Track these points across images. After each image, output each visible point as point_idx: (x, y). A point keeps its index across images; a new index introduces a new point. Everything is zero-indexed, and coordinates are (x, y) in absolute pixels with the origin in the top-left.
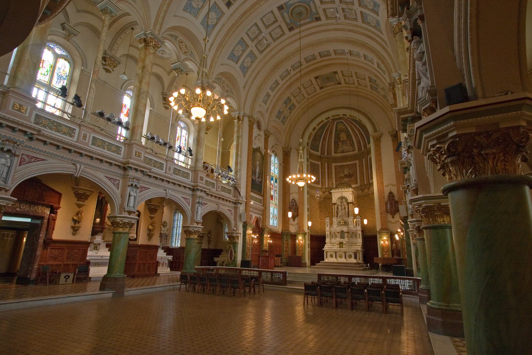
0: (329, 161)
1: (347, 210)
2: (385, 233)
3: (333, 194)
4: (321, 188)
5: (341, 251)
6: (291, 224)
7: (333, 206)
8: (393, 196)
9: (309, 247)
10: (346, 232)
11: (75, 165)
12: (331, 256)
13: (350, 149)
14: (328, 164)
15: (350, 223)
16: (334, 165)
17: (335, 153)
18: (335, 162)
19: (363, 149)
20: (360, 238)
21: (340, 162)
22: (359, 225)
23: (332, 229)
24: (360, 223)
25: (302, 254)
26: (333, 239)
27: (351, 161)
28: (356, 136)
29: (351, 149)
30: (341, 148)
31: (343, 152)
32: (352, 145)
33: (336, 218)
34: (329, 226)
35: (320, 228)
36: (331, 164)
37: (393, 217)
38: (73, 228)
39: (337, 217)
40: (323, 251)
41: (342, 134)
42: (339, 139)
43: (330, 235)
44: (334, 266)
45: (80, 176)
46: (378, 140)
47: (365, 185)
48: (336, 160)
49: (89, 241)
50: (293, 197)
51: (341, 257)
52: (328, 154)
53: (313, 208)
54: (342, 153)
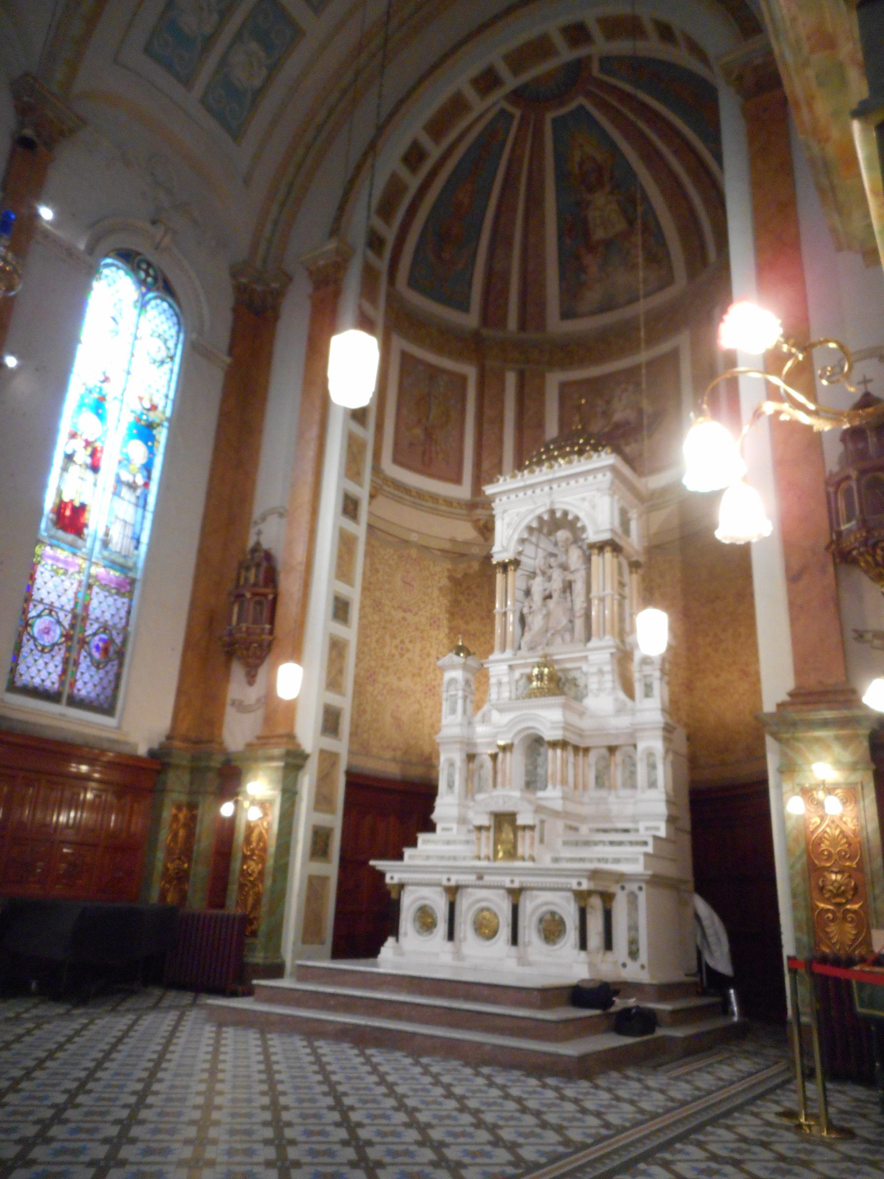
3: (498, 507)
5: (488, 879)
6: (233, 704)
7: (499, 577)
10: (554, 745)
15: (593, 683)
17: (567, 314)
18: (563, 366)
20: (652, 784)
22: (648, 693)
24: (657, 674)
31: (607, 306)
36: (542, 377)
41: (599, 199)
42: (586, 233)
52: (523, 326)
53: (399, 614)
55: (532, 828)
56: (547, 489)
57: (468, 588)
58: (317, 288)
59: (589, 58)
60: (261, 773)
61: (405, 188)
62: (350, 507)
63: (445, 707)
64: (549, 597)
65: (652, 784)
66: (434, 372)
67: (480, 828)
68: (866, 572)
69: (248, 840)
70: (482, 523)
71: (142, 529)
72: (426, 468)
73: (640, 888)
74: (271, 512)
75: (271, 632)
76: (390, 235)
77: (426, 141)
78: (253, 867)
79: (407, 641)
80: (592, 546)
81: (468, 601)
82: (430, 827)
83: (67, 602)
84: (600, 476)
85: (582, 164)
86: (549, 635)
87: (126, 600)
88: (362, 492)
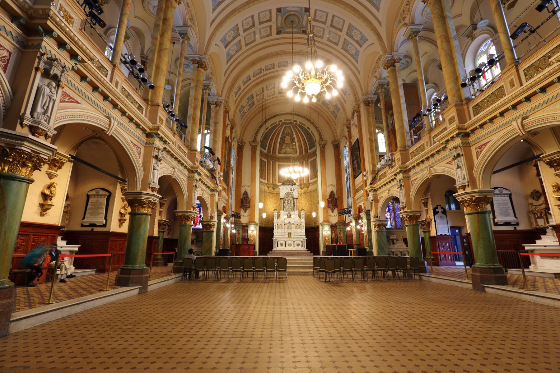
1: (292, 205)
4: (267, 184)
8: (334, 194)
11: (108, 118)
12: (282, 245)
17: (279, 153)
19: (304, 153)
23: (279, 221)
28: (299, 141)
31: (285, 153)
37: (333, 212)
38: (42, 205)
45: (111, 135)
46: (323, 148)
47: (305, 184)
49: (60, 225)
51: (290, 245)
52: (273, 154)
80: (295, 198)
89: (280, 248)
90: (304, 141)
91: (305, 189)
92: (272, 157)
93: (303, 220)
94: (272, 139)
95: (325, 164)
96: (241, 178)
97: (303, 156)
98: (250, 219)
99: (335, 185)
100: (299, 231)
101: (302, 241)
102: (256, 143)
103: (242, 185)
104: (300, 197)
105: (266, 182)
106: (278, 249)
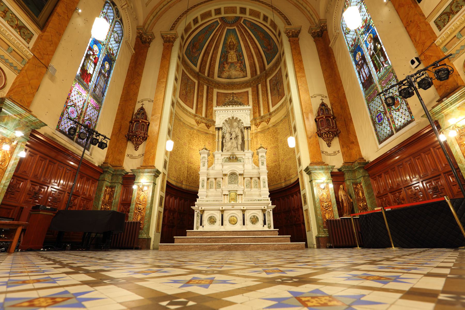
0: (209, 84)
1: (240, 141)
2: (323, 169)
5: (236, 207)
9: (160, 204)
10: (240, 175)
12: (212, 220)
13: (239, 74)
14: (208, 87)
15: (246, 161)
16: (215, 91)
18: (218, 88)
19: (258, 73)
20: (264, 187)
21: (225, 89)
22: (263, 163)
25: (142, 218)
26: (211, 190)
27: (240, 88)
28: (250, 57)
29: (242, 74)
30: (227, 72)
31: (229, 77)
32: (243, 69)
33: (220, 151)
34: (206, 164)
35: (187, 177)
37: (329, 145)
39: (222, 151)
40: (193, 211)
41: (232, 52)
43: (207, 183)
44: (227, 240)
47: (262, 117)
48: (219, 85)
50: (143, 104)
51: (233, 222)
52: (208, 76)
54: (228, 78)
55: (242, 195)
56: (231, 111)
57: (193, 137)
58: (165, 42)
59: (242, 17)
60: (144, 177)
61: (191, 28)
62: (173, 104)
63: (201, 165)
64: (231, 139)
65: (264, 187)
66: (189, 79)
67: (225, 195)
68: (323, 139)
69: (138, 198)
70: (197, 121)
71: (105, 91)
72: (185, 102)
73: (271, 210)
74: (146, 100)
75: (147, 134)
76: (185, 38)
77: (199, 19)
78: (141, 206)
79: (179, 147)
81: (193, 140)
82: (198, 197)
83: (80, 104)
84: (247, 111)
85: (230, 42)
86: (232, 148)
87: (97, 112)
88: (175, 101)
89: (207, 227)
90: (258, 54)
91: (264, 124)
92: (207, 79)
93: (264, 170)
94: (207, 53)
95: (301, 61)
96: (138, 88)
97: (258, 78)
98: (145, 161)
99: (326, 94)
100: (255, 191)
101: (263, 211)
102: (173, 32)
103: (139, 99)
104: (255, 140)
105: (193, 111)
106: (201, 229)
